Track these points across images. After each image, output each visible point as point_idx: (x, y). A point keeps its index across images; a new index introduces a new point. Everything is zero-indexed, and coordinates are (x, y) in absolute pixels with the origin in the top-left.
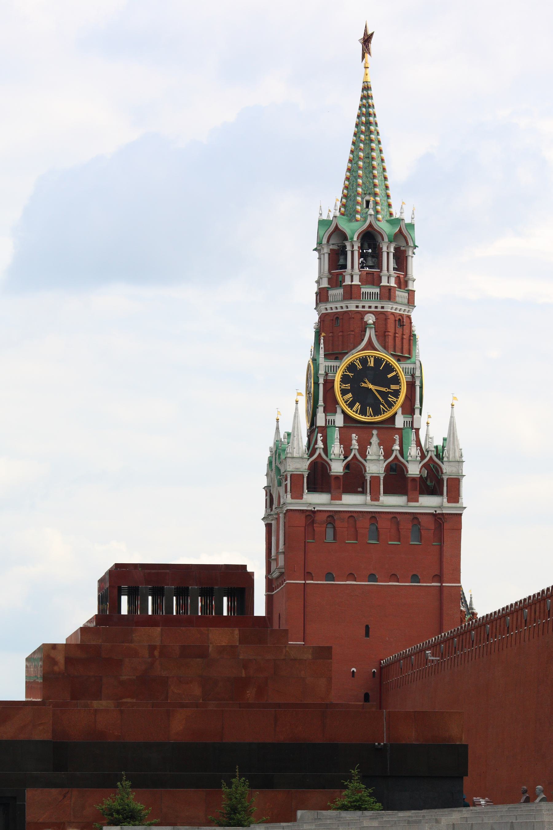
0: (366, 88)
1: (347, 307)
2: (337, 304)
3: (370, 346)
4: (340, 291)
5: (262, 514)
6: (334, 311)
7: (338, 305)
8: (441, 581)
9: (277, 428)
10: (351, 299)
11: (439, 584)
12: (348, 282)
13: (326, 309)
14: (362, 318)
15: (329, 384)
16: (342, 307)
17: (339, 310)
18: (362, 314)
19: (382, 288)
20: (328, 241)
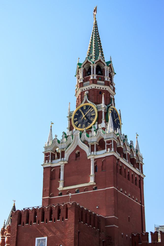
0: (96, 25)
1: (106, 89)
2: (100, 86)
3: (112, 105)
4: (103, 82)
5: (43, 162)
6: (99, 88)
7: (102, 87)
8: (141, 203)
9: (51, 130)
10: (108, 86)
11: (141, 205)
12: (106, 79)
13: (95, 87)
14: (110, 95)
15: (106, 114)
16: (103, 88)
17: (102, 89)
18: (110, 94)
19: (113, 87)
20: (96, 63)
